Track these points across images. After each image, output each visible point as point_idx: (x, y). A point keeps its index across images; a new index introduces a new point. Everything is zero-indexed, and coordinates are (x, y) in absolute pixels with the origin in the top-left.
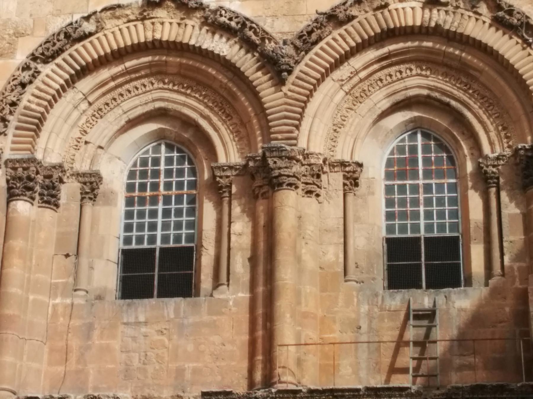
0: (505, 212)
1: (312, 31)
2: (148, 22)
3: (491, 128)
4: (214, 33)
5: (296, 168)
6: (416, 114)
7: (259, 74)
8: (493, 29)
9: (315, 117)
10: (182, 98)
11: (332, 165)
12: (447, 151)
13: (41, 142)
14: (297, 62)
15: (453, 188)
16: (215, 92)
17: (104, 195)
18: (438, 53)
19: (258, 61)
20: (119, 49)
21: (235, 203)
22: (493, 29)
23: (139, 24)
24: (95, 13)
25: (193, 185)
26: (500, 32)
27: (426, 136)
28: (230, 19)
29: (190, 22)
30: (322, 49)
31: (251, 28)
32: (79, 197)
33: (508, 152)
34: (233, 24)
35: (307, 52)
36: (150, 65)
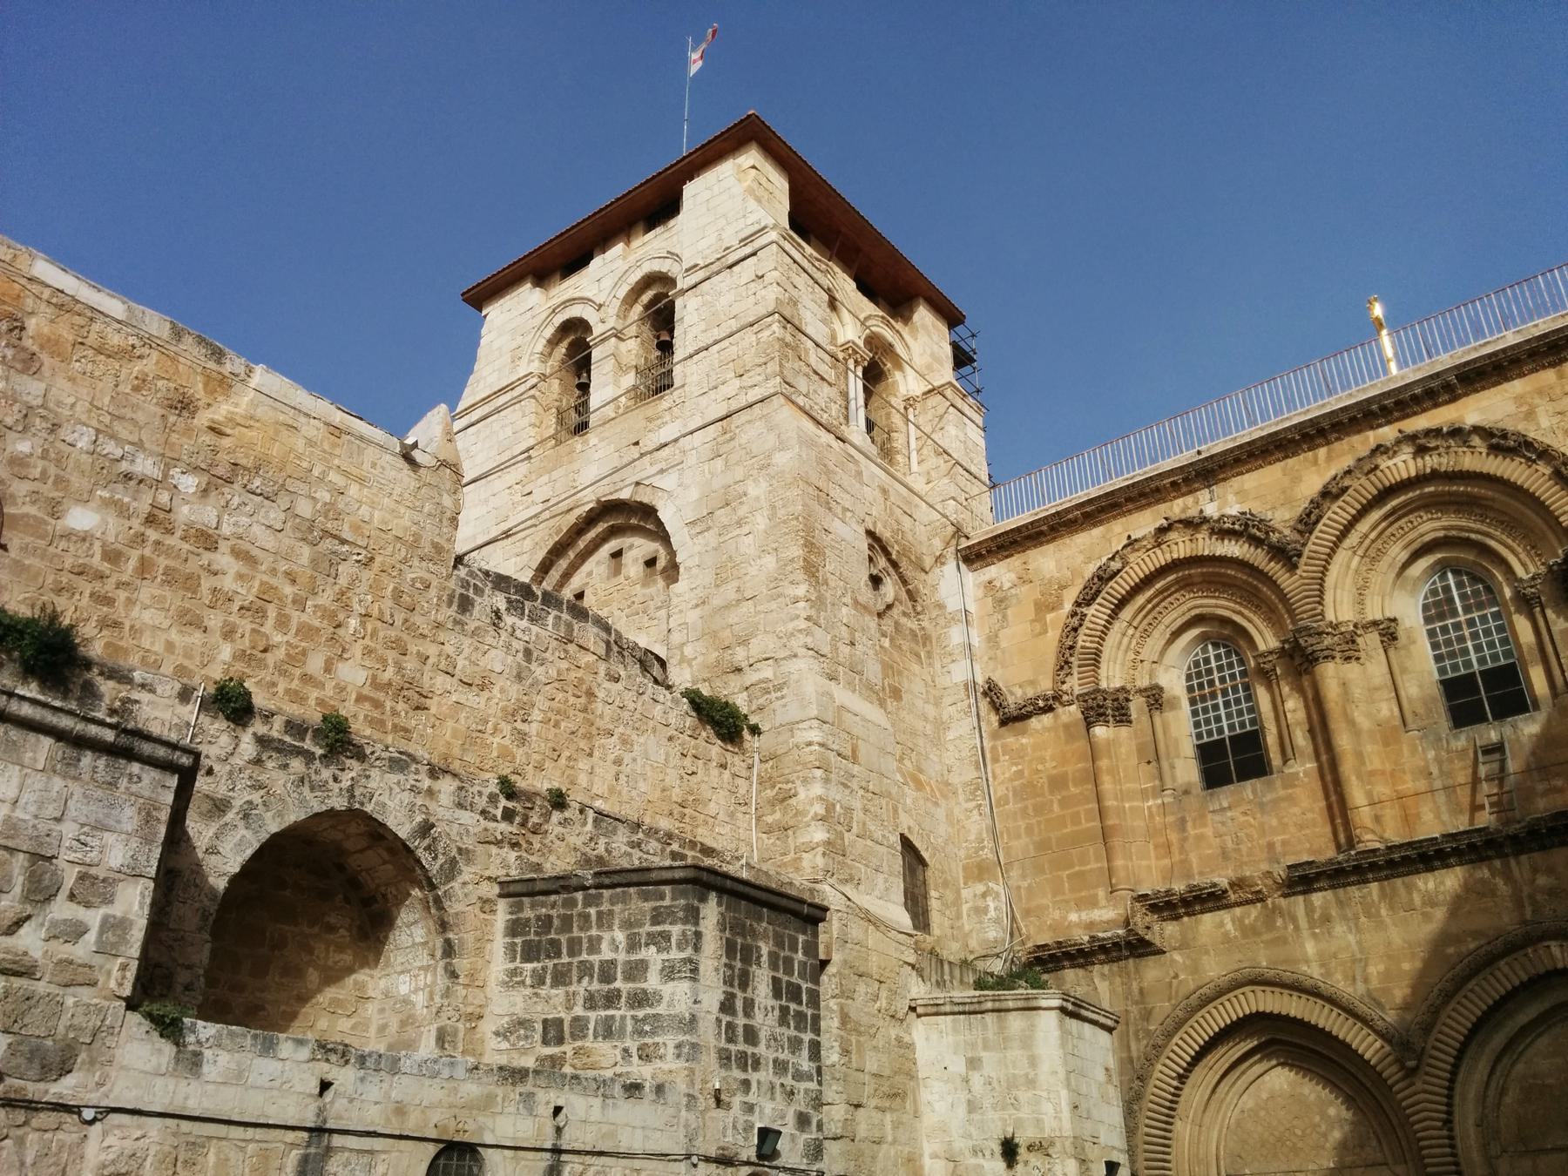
0: (1555, 629)
1: (1311, 512)
2: (1164, 546)
3: (1520, 550)
4: (1223, 540)
5: (1328, 641)
6: (1439, 556)
7: (1272, 564)
8: (1492, 457)
9: (1335, 588)
10: (1213, 601)
11: (1365, 627)
12: (1482, 581)
13: (1103, 672)
14: (1304, 545)
15: (1497, 616)
16: (1239, 588)
17: (1169, 701)
18: (1443, 494)
19: (1268, 553)
20: (1146, 576)
21: (1282, 683)
22: (1492, 457)
23: (1158, 551)
24: (1117, 552)
25: (1244, 674)
26: (1500, 458)
27: (1456, 573)
28: (1233, 524)
29: (1199, 536)
30: (1325, 525)
31: (1254, 526)
32: (1147, 709)
33: (1543, 569)
34: (1237, 527)
35: (1311, 533)
36: (1177, 581)
